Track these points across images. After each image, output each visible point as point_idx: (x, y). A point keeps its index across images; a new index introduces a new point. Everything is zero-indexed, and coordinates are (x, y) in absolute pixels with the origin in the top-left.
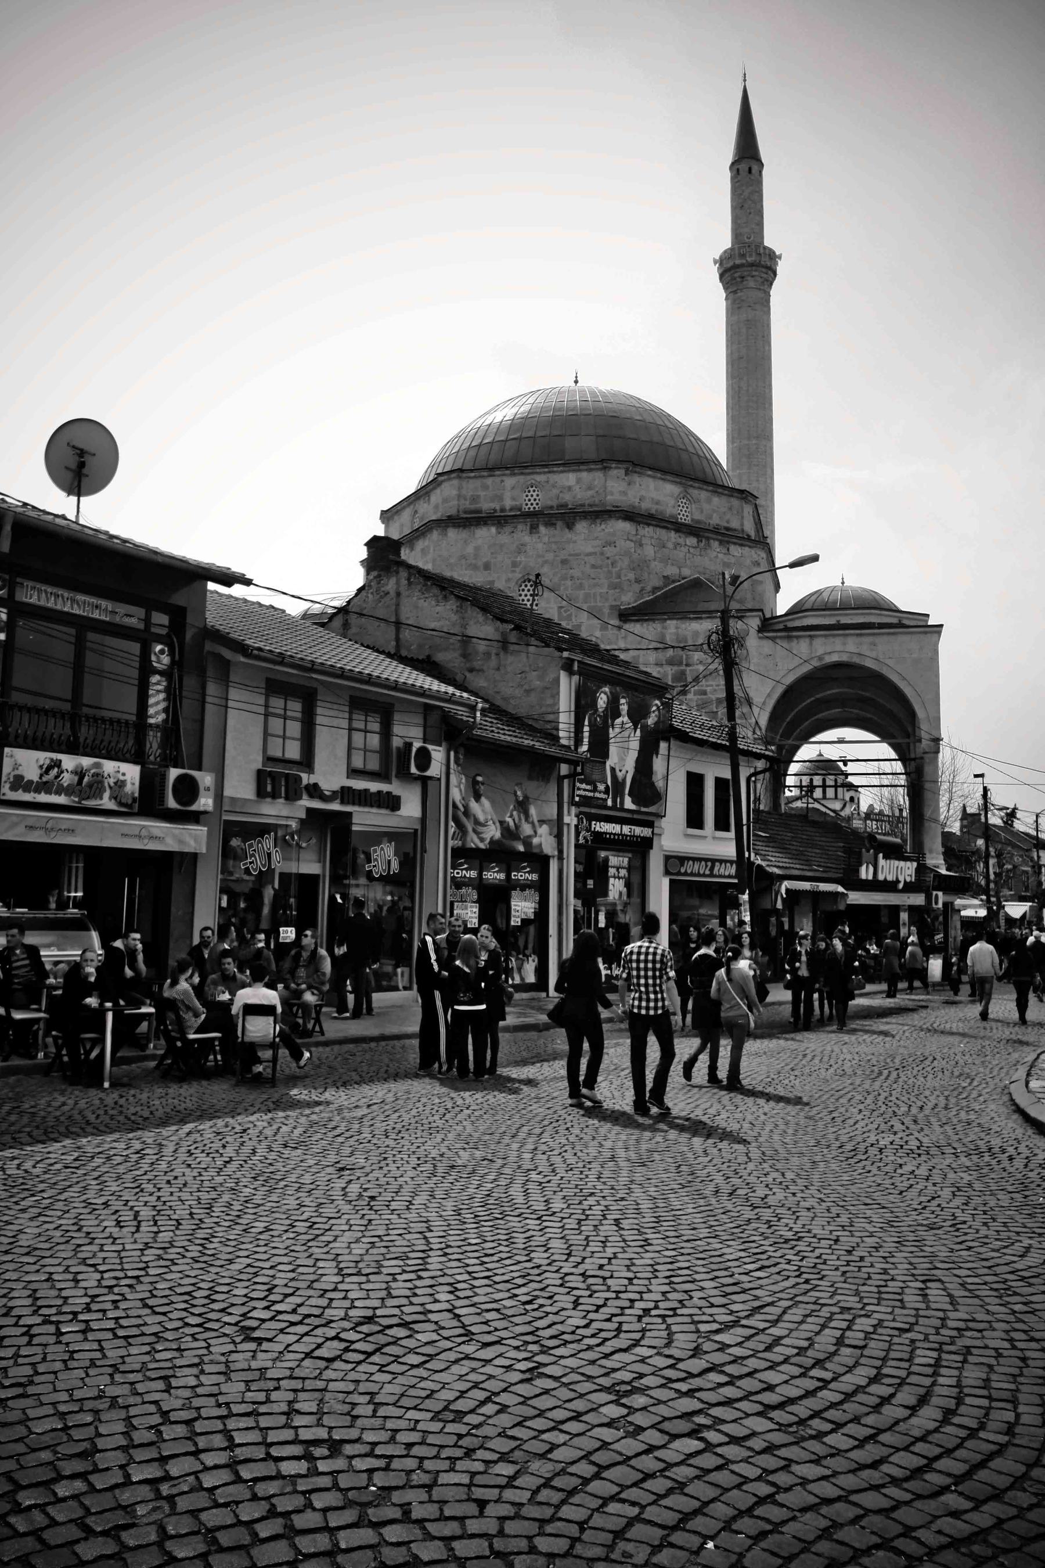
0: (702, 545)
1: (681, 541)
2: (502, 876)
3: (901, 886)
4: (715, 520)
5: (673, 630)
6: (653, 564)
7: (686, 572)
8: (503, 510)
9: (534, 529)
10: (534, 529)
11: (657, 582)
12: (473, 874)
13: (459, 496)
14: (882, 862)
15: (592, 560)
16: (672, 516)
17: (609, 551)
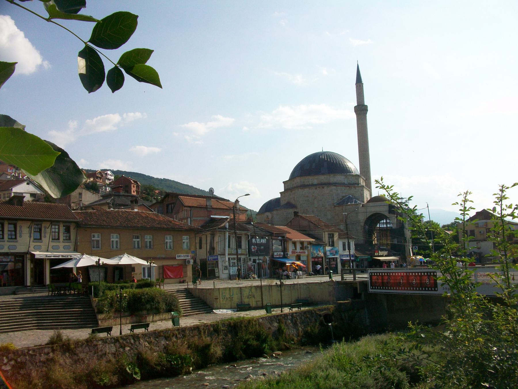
1: (346, 188)
4: (353, 182)
7: (347, 194)
8: (310, 184)
9: (316, 188)
11: (341, 197)
13: (301, 182)
14: (379, 252)
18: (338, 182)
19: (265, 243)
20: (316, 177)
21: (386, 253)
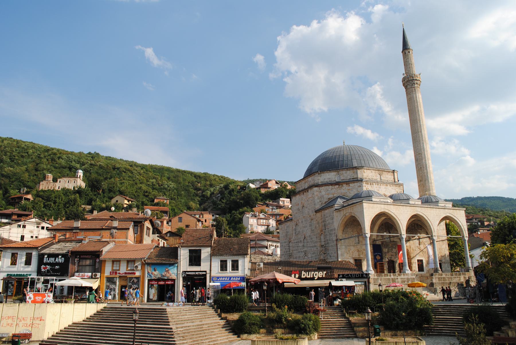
0: (340, 187)
1: (333, 187)
2: (164, 283)
3: (315, 279)
4: (349, 177)
5: (323, 214)
6: (325, 196)
7: (335, 195)
10: (303, 193)
11: (326, 200)
12: (156, 283)
14: (303, 273)
15: (311, 199)
16: (334, 181)
17: (313, 196)
18: (325, 181)
19: (62, 262)
20: (307, 180)
21: (321, 274)
